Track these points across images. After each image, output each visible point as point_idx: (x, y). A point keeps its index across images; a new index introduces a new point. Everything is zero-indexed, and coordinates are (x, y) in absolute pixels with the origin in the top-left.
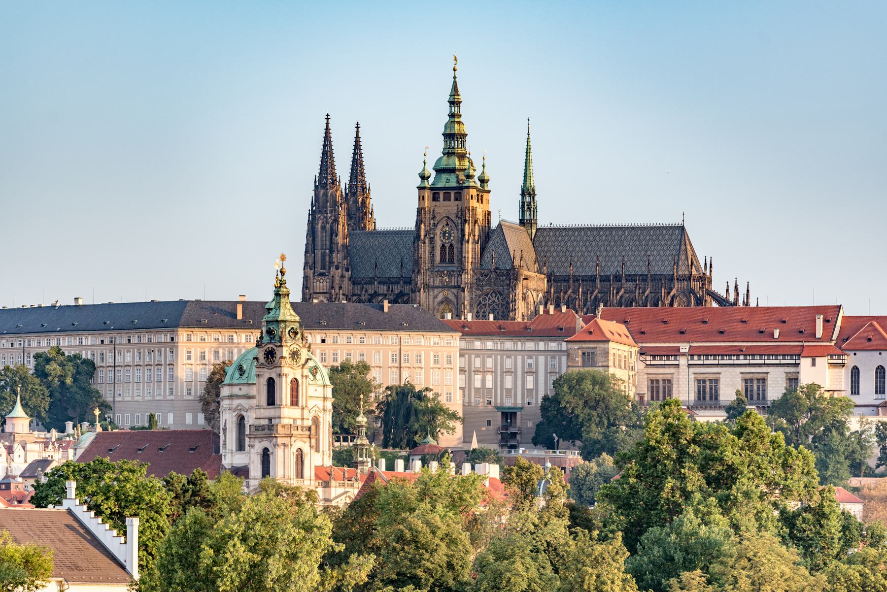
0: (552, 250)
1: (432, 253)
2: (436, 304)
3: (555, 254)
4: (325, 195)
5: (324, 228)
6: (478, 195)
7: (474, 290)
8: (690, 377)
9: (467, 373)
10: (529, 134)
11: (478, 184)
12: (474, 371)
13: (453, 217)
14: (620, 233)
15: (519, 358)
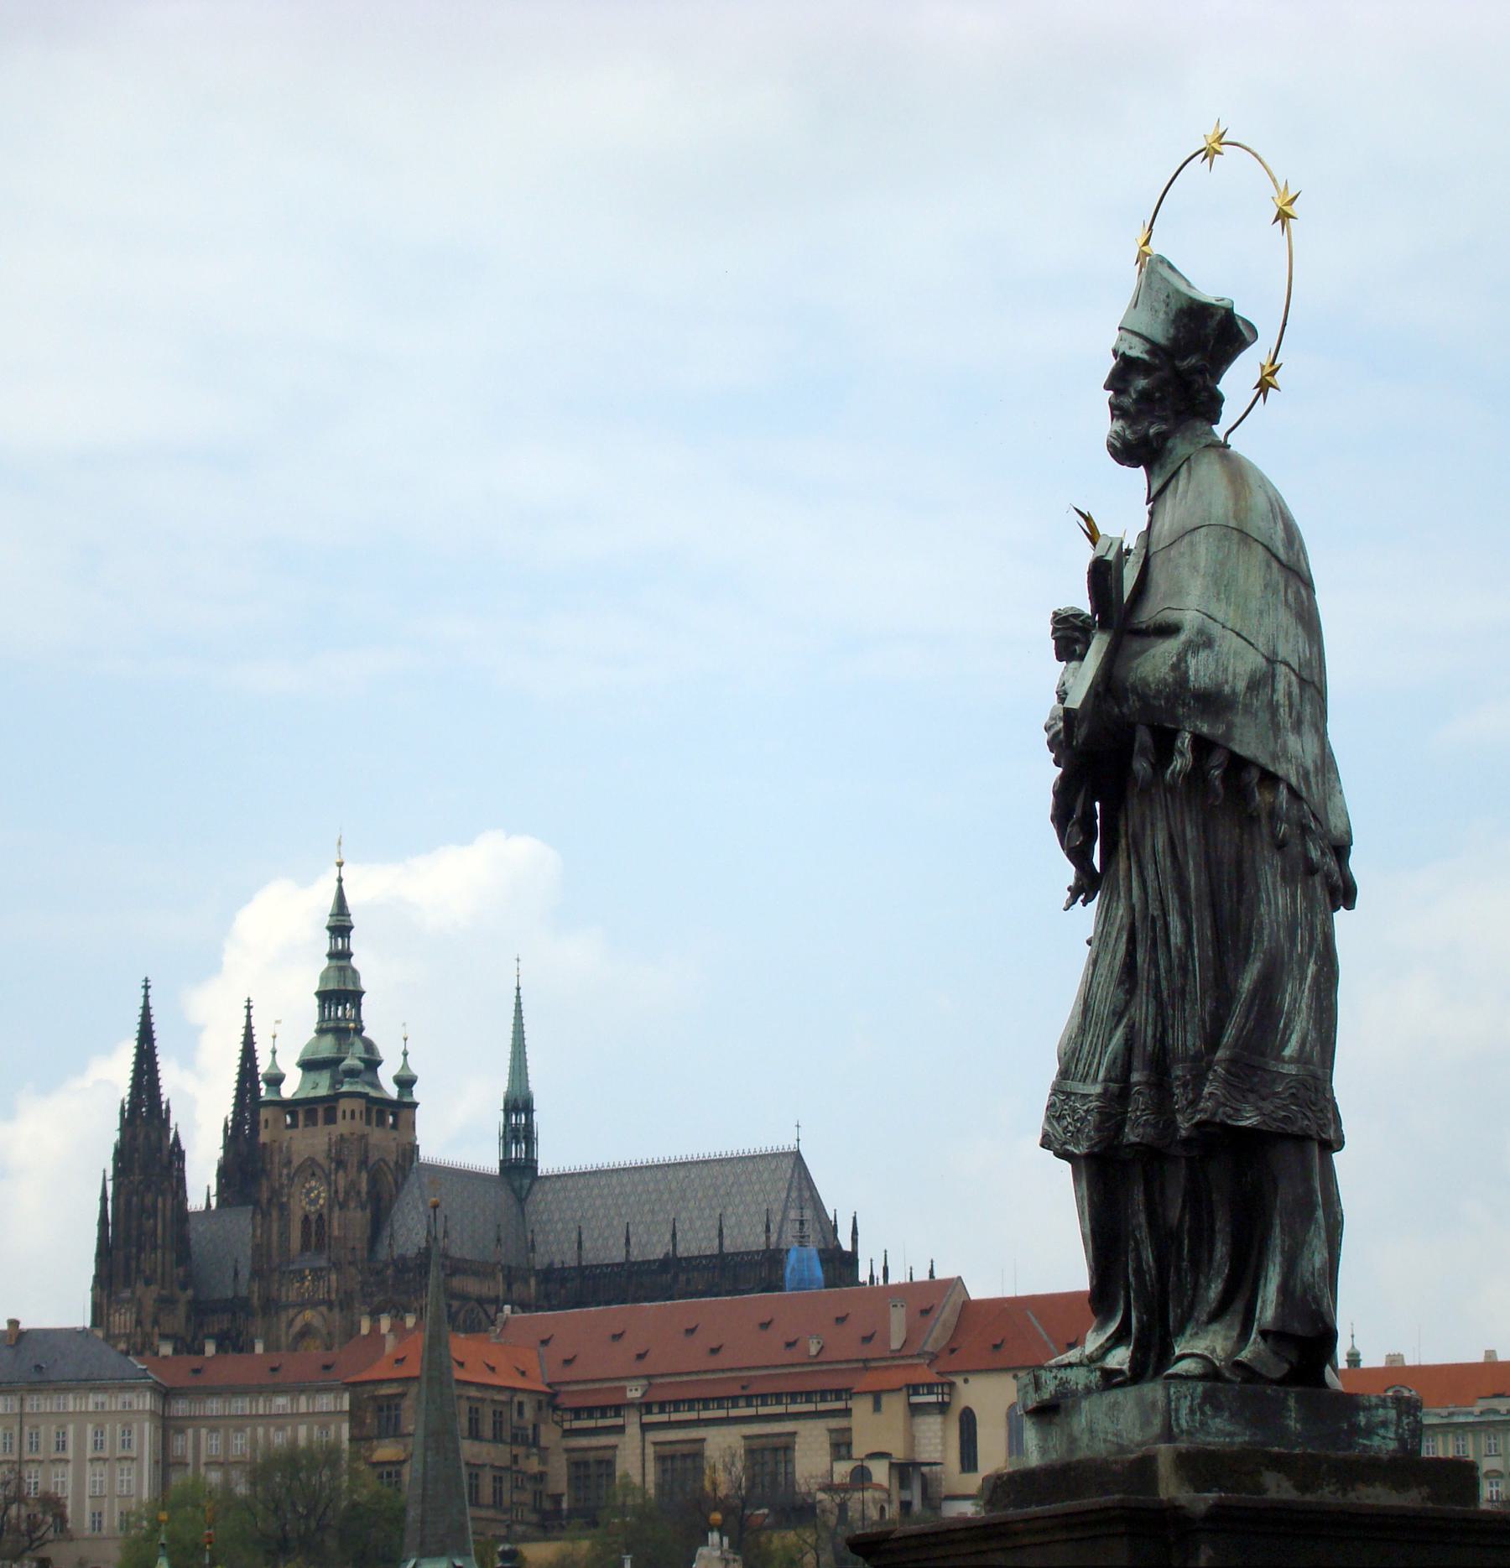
0: (556, 1219)
1: (284, 1234)
2: (290, 1338)
3: (560, 1226)
4: (134, 1137)
5: (128, 1203)
6: (368, 1110)
7: (357, 1305)
8: (646, 1451)
9: (190, 1470)
10: (518, 989)
11: (392, 1091)
12: (207, 1464)
13: (321, 1158)
14: (682, 1174)
15: (302, 1431)
